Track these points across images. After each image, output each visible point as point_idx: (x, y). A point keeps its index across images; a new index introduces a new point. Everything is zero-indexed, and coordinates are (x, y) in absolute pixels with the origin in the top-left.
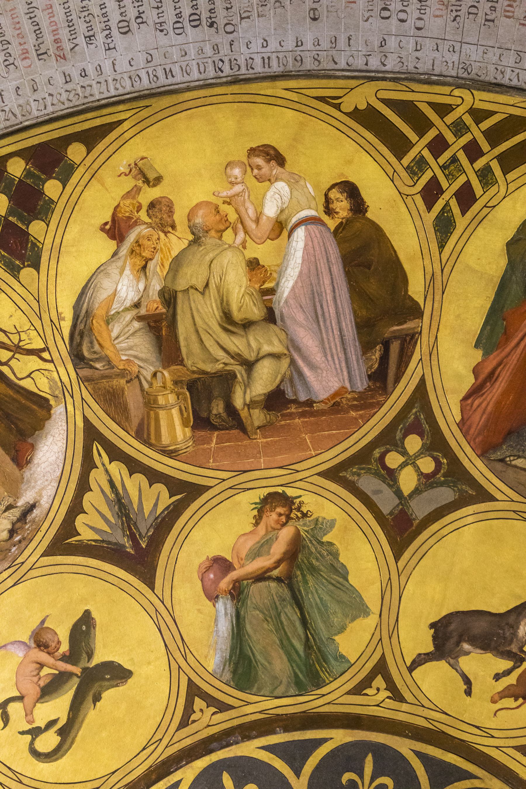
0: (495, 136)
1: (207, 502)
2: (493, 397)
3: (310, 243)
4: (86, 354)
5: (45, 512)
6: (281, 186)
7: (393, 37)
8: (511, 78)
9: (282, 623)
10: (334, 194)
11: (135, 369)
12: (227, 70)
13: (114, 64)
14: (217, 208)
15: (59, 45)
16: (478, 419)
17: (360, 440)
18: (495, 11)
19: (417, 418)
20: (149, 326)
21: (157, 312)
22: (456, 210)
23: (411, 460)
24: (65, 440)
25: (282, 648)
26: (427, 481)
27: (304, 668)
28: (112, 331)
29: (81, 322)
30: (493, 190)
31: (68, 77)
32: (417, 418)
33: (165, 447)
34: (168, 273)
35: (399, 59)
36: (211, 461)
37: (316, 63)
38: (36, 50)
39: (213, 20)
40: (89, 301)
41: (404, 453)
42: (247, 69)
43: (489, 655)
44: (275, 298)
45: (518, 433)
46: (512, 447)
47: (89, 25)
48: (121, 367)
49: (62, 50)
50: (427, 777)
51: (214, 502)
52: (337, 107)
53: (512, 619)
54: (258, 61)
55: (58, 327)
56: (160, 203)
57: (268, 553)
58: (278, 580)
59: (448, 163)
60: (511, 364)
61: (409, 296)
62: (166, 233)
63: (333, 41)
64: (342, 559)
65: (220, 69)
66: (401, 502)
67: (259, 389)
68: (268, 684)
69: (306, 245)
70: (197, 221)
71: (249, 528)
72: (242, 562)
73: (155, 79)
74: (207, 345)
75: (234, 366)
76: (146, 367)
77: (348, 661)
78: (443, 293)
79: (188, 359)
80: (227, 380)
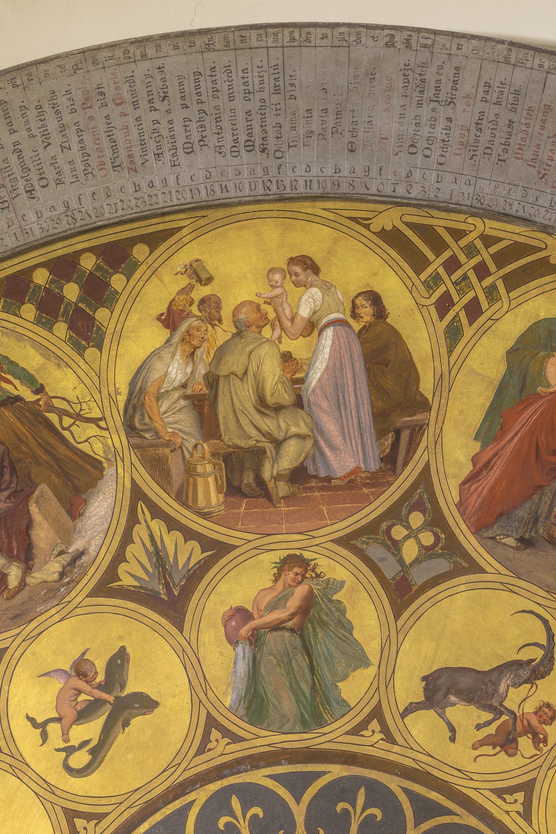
0: (501, 259)
1: (234, 559)
2: (488, 483)
3: (337, 342)
4: (137, 425)
5: (92, 559)
6: (315, 292)
7: (418, 170)
8: (518, 210)
9: (292, 668)
10: (360, 301)
11: (179, 441)
12: (274, 189)
13: (177, 179)
14: (258, 306)
15: (132, 159)
16: (474, 502)
17: (370, 513)
18: (507, 152)
19: (421, 498)
20: (194, 404)
21: (201, 392)
22: (464, 321)
23: (413, 534)
24: (114, 498)
25: (291, 691)
27: (309, 709)
28: (161, 405)
29: (135, 397)
30: (499, 304)
31: (137, 187)
32: (421, 498)
33: (200, 510)
34: (212, 360)
35: (422, 189)
36: (240, 524)
37: (351, 188)
38: (112, 163)
39: (265, 146)
40: (143, 380)
41: (408, 527)
42: (292, 190)
43: (473, 707)
44: (303, 387)
45: (508, 515)
47: (159, 144)
48: (167, 438)
49: (134, 164)
51: (240, 559)
52: (367, 227)
53: (494, 677)
54: (301, 182)
55: (115, 400)
56: (210, 299)
57: (285, 607)
58: (292, 630)
59: (459, 280)
60: (505, 456)
61: (420, 392)
62: (213, 326)
63: (367, 170)
64: (348, 616)
65: (268, 188)
66: (403, 570)
67: (285, 464)
68: (277, 721)
69: (333, 343)
70: (241, 317)
71: (269, 584)
72: (261, 613)
73: (212, 192)
74: (243, 424)
75: (265, 443)
76: (188, 440)
78: (450, 391)
79: (225, 435)
80: (257, 455)
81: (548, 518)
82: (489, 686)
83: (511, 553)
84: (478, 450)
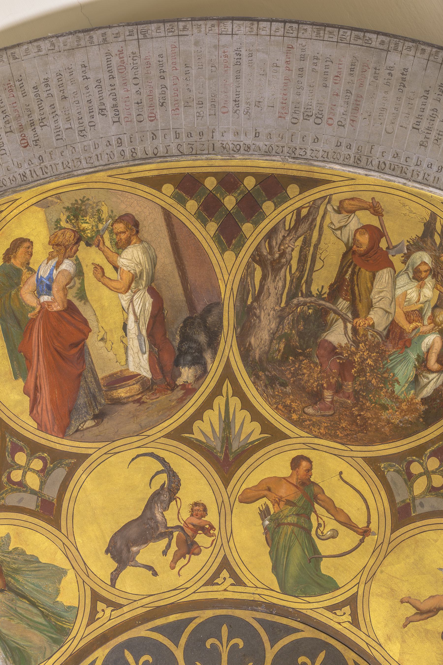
2: (46, 399)
9: (21, 614)
16: (47, 418)
19: (12, 443)
23: (26, 469)
26: (44, 474)
27: (52, 631)
32: (12, 443)
41: (20, 467)
43: (151, 543)
45: (75, 409)
46: (78, 419)
50: (167, 639)
53: (148, 514)
64: (28, 553)
66: (38, 496)
68: (39, 654)
77: (74, 607)
81: (100, 390)
82: (150, 523)
83: (96, 430)
84: (23, 384)
